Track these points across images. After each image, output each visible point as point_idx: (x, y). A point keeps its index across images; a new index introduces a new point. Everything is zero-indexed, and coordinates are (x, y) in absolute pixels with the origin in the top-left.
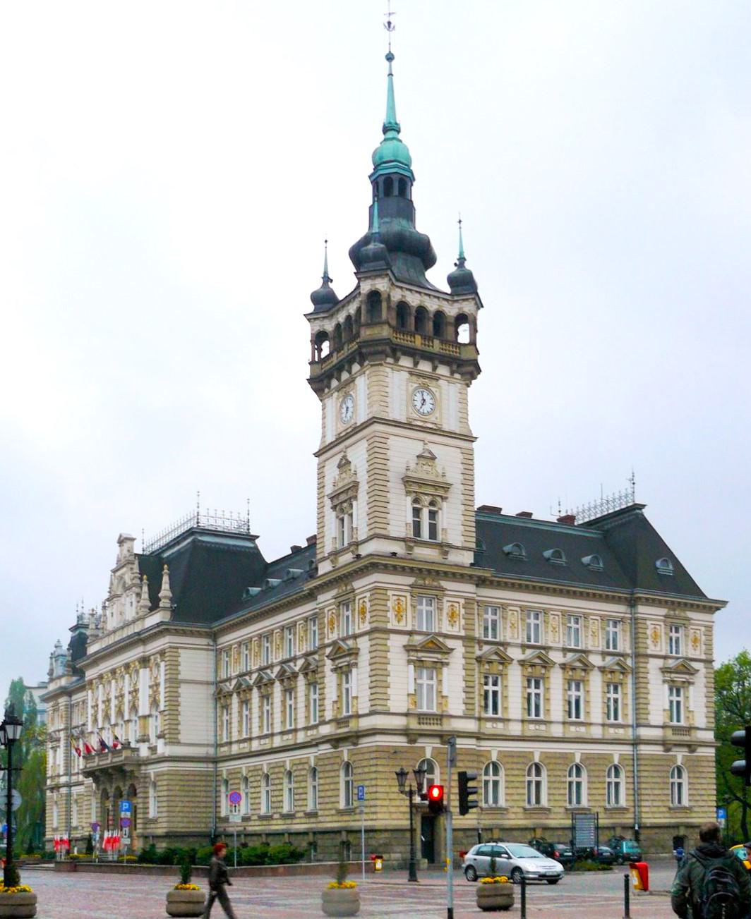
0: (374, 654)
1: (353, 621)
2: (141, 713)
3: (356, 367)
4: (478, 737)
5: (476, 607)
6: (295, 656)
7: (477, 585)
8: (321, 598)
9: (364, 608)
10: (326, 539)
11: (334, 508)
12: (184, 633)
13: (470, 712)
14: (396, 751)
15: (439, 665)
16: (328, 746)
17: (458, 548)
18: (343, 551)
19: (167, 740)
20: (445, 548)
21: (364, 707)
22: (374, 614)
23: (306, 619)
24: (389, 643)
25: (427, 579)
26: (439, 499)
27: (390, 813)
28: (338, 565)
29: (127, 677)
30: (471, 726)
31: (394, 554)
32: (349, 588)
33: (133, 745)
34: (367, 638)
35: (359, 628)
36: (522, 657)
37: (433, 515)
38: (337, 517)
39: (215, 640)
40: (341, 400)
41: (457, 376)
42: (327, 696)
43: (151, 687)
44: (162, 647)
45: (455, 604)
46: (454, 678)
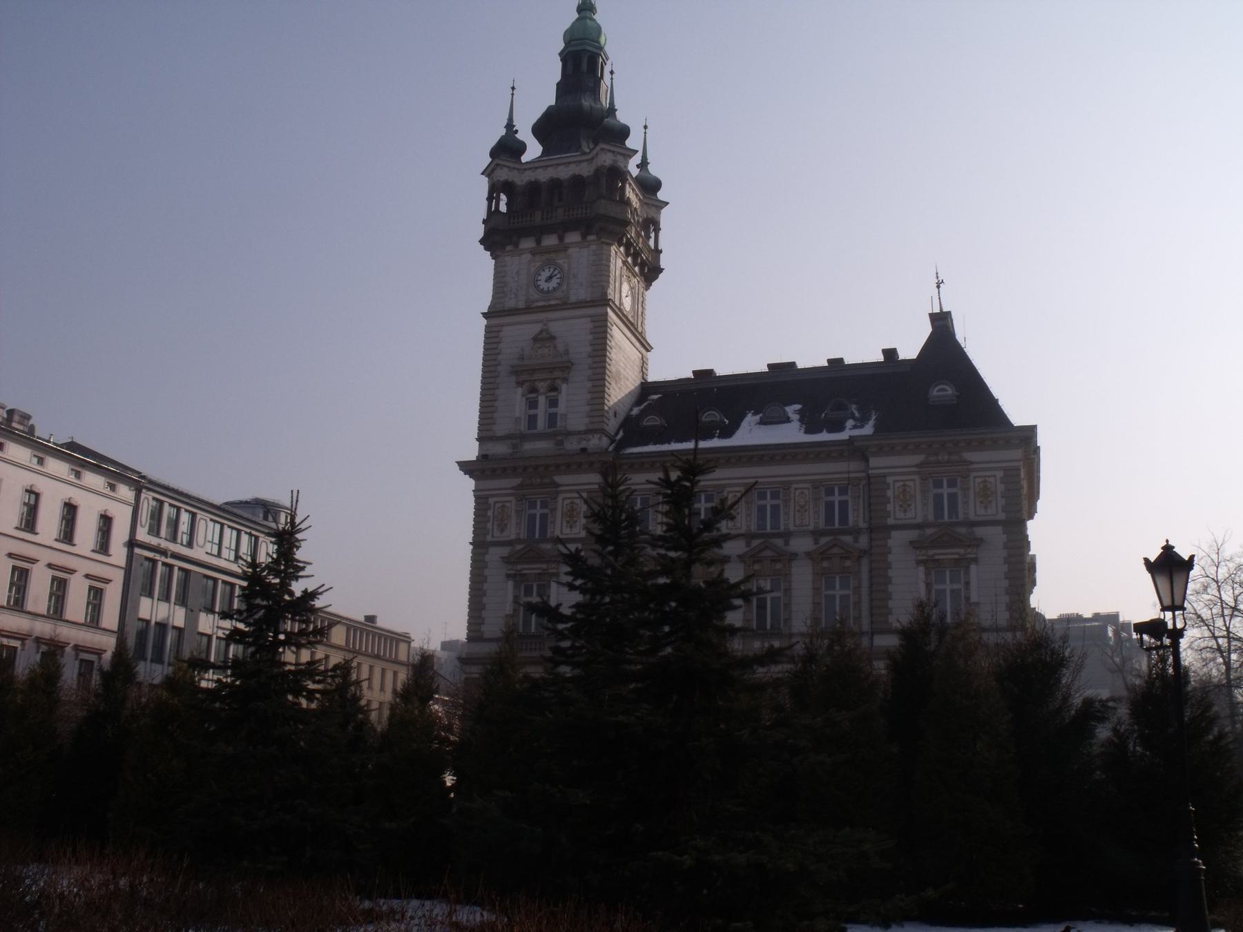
37: (553, 403)
41: (591, 238)
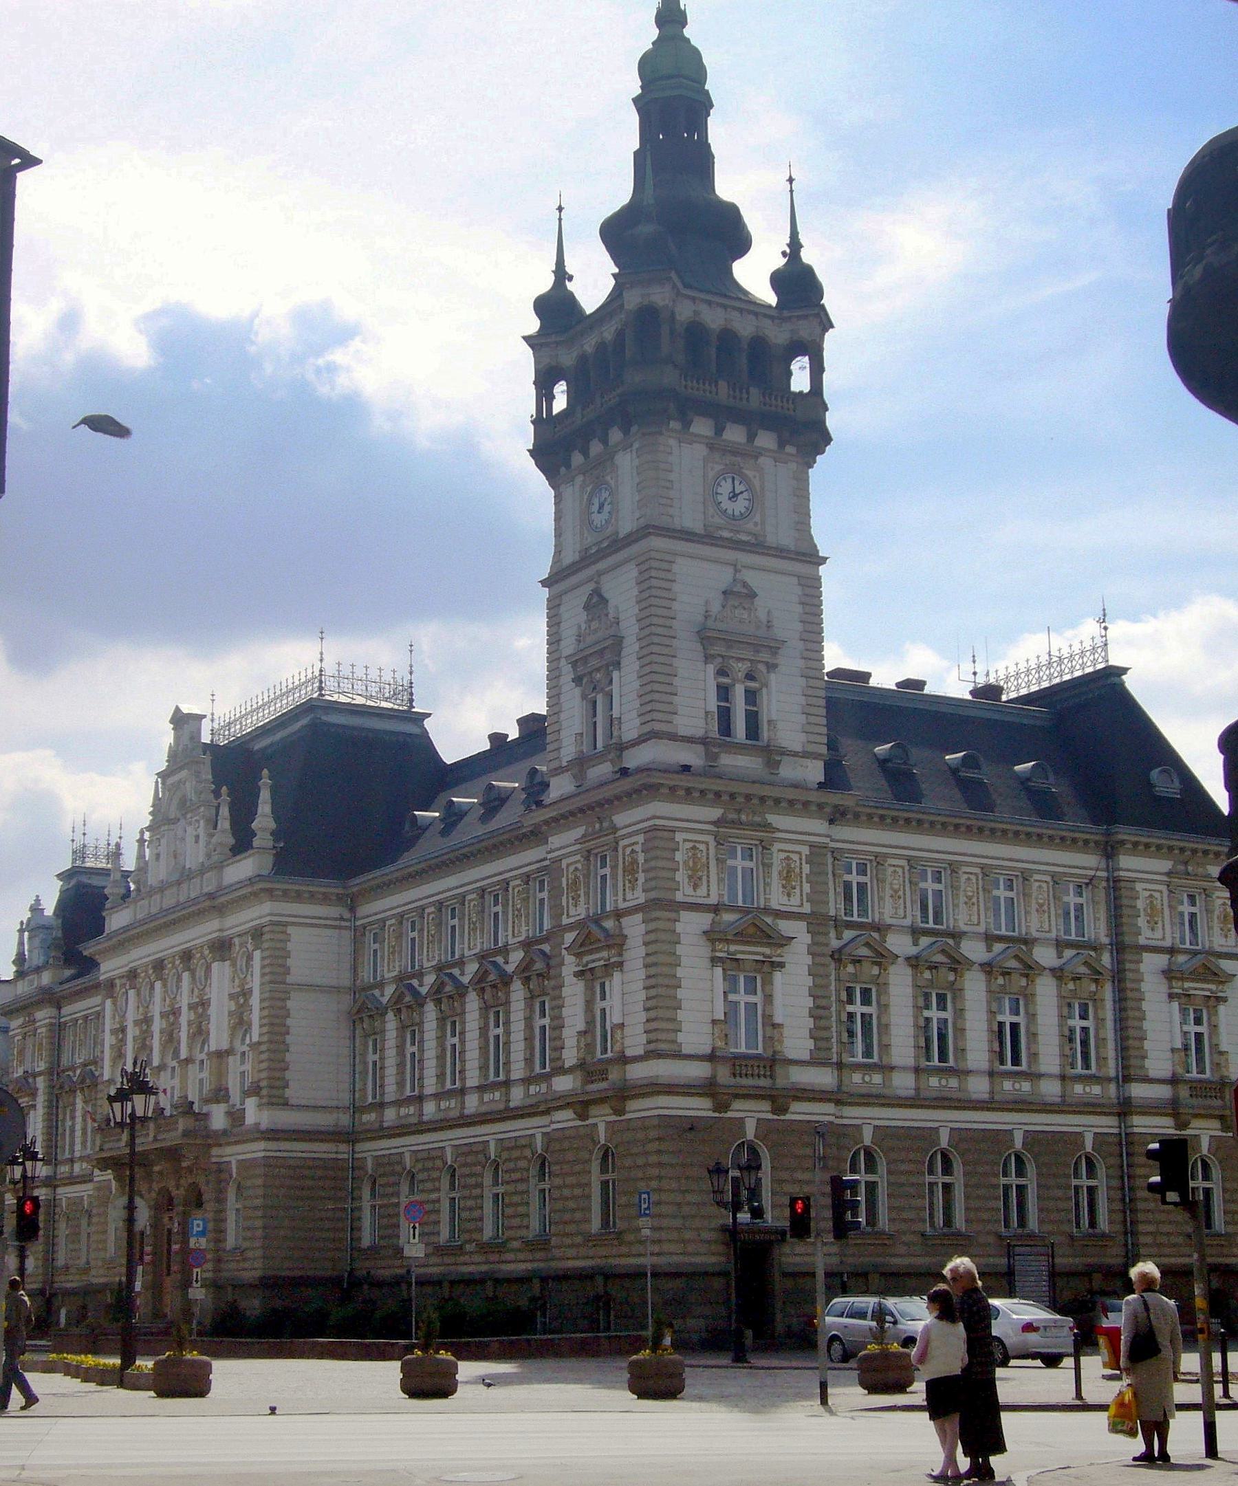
0: (652, 948)
1: (615, 886)
2: (213, 1046)
3: (615, 435)
4: (837, 1097)
5: (830, 860)
6: (506, 945)
7: (831, 822)
8: (555, 841)
9: (634, 862)
10: (563, 733)
11: (578, 680)
12: (298, 897)
13: (822, 1054)
14: (692, 1126)
15: (766, 968)
16: (568, 1114)
17: (795, 754)
18: (598, 758)
19: (265, 1100)
20: (772, 755)
21: (635, 1042)
22: (652, 875)
23: (527, 878)
24: (679, 927)
25: (745, 811)
26: (762, 667)
27: (683, 1241)
28: (588, 784)
29: (186, 976)
30: (824, 1078)
31: (686, 768)
32: (605, 824)
33: (196, 1108)
34: (639, 917)
35: (624, 900)
36: (913, 951)
38: (584, 697)
39: (352, 909)
40: (589, 489)
41: (790, 449)
42: (567, 1022)
43: (232, 997)
44: (258, 922)
45: (792, 855)
46: (792, 994)
